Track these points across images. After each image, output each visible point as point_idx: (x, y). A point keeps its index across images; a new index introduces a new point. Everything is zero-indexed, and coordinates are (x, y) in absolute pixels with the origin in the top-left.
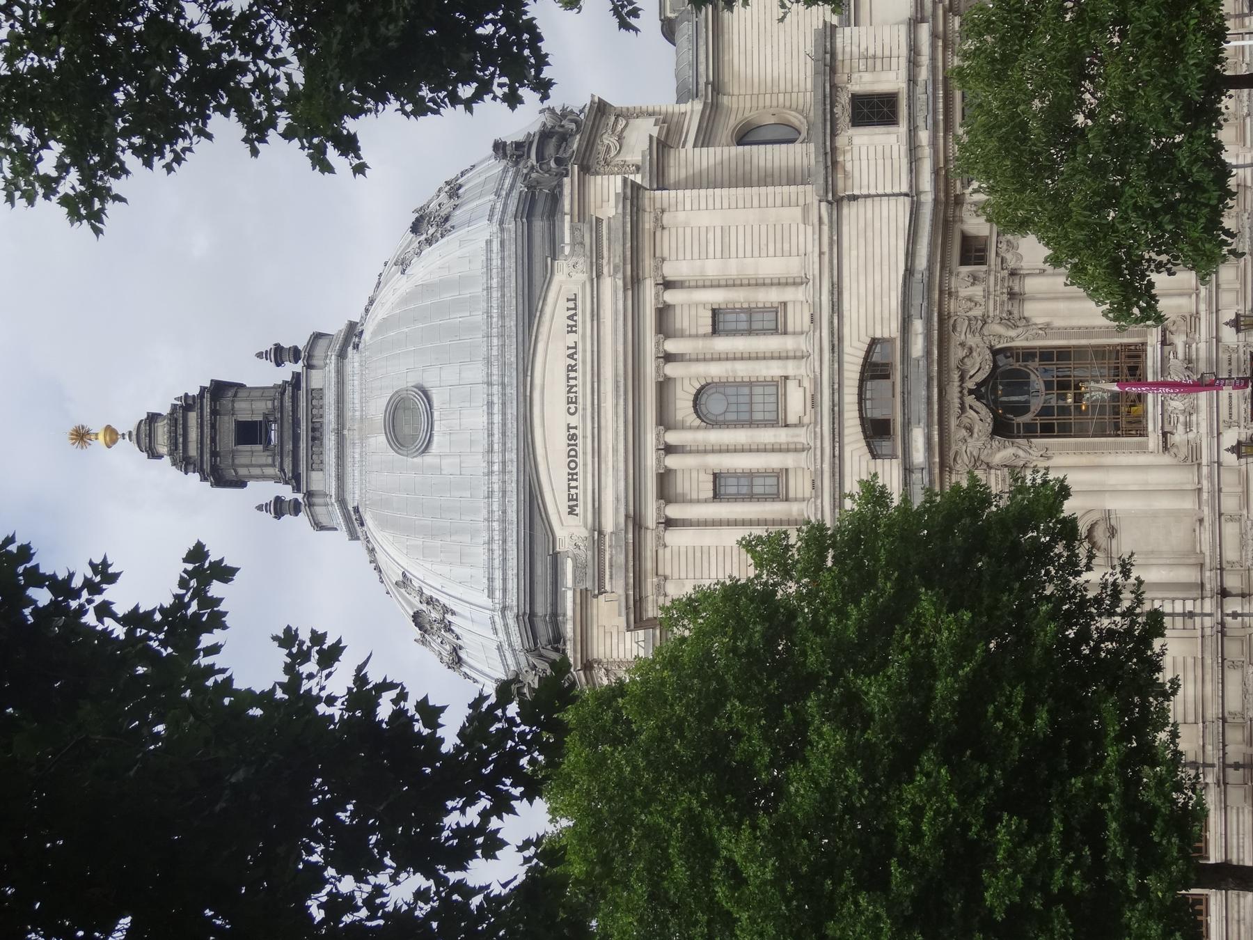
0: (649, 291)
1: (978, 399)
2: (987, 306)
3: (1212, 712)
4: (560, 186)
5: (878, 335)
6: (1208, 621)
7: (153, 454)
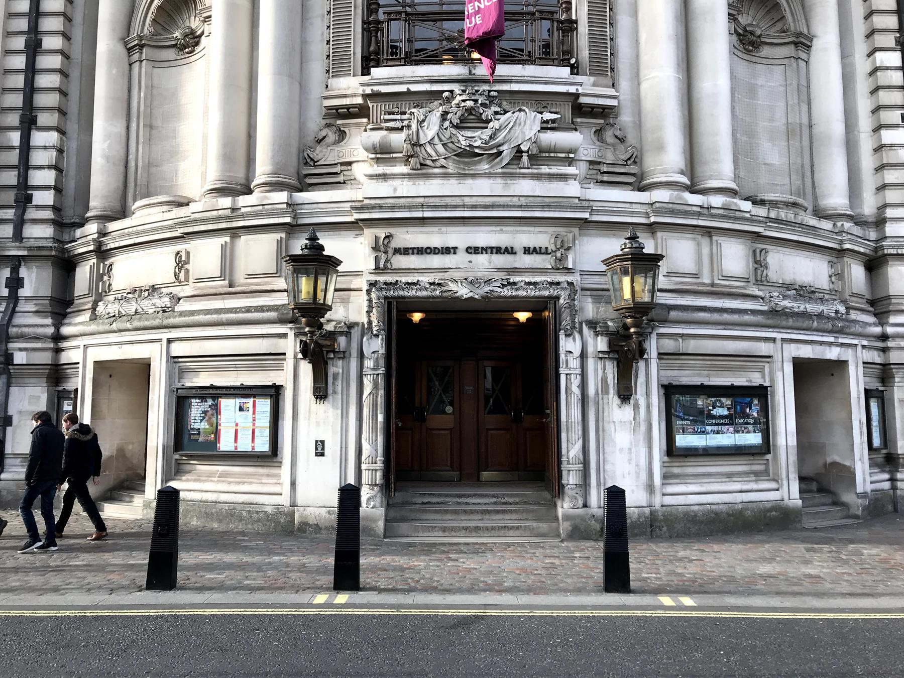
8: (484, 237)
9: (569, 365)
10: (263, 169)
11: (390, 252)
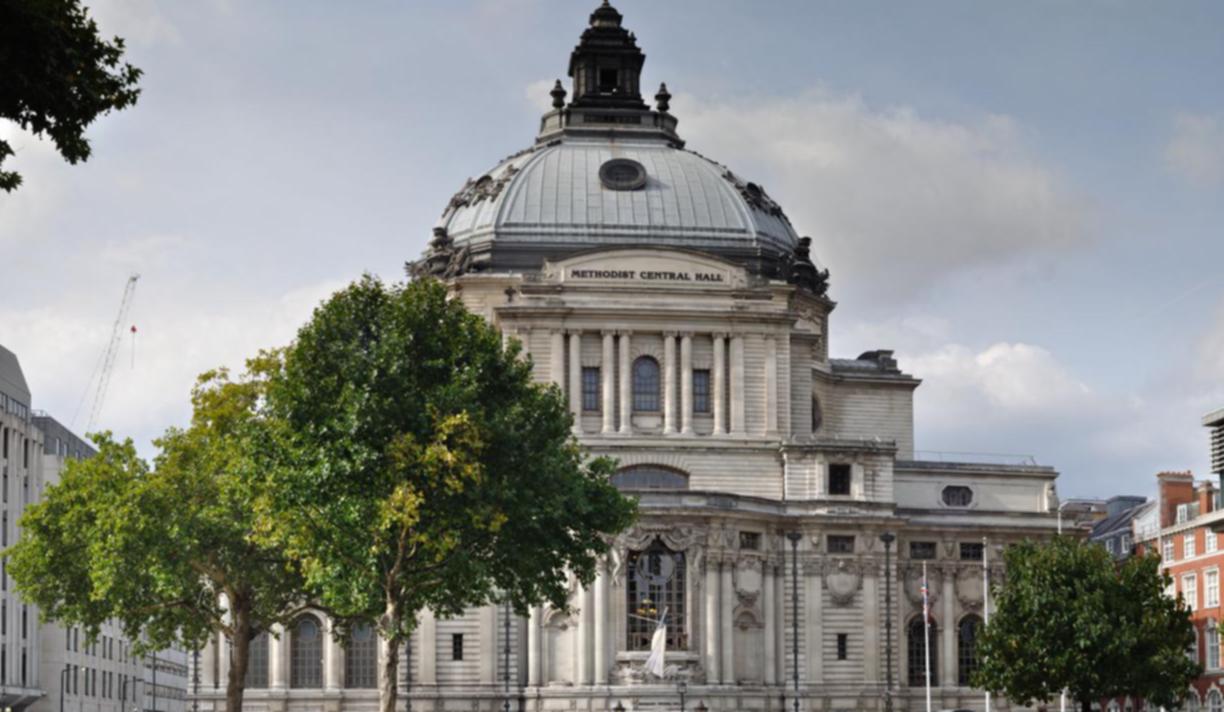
0: (724, 328)
1: (654, 542)
3: (445, 692)
4: (781, 279)
5: (692, 478)
6: (503, 689)
7: (593, 18)
8: (663, 700)
10: (598, 678)
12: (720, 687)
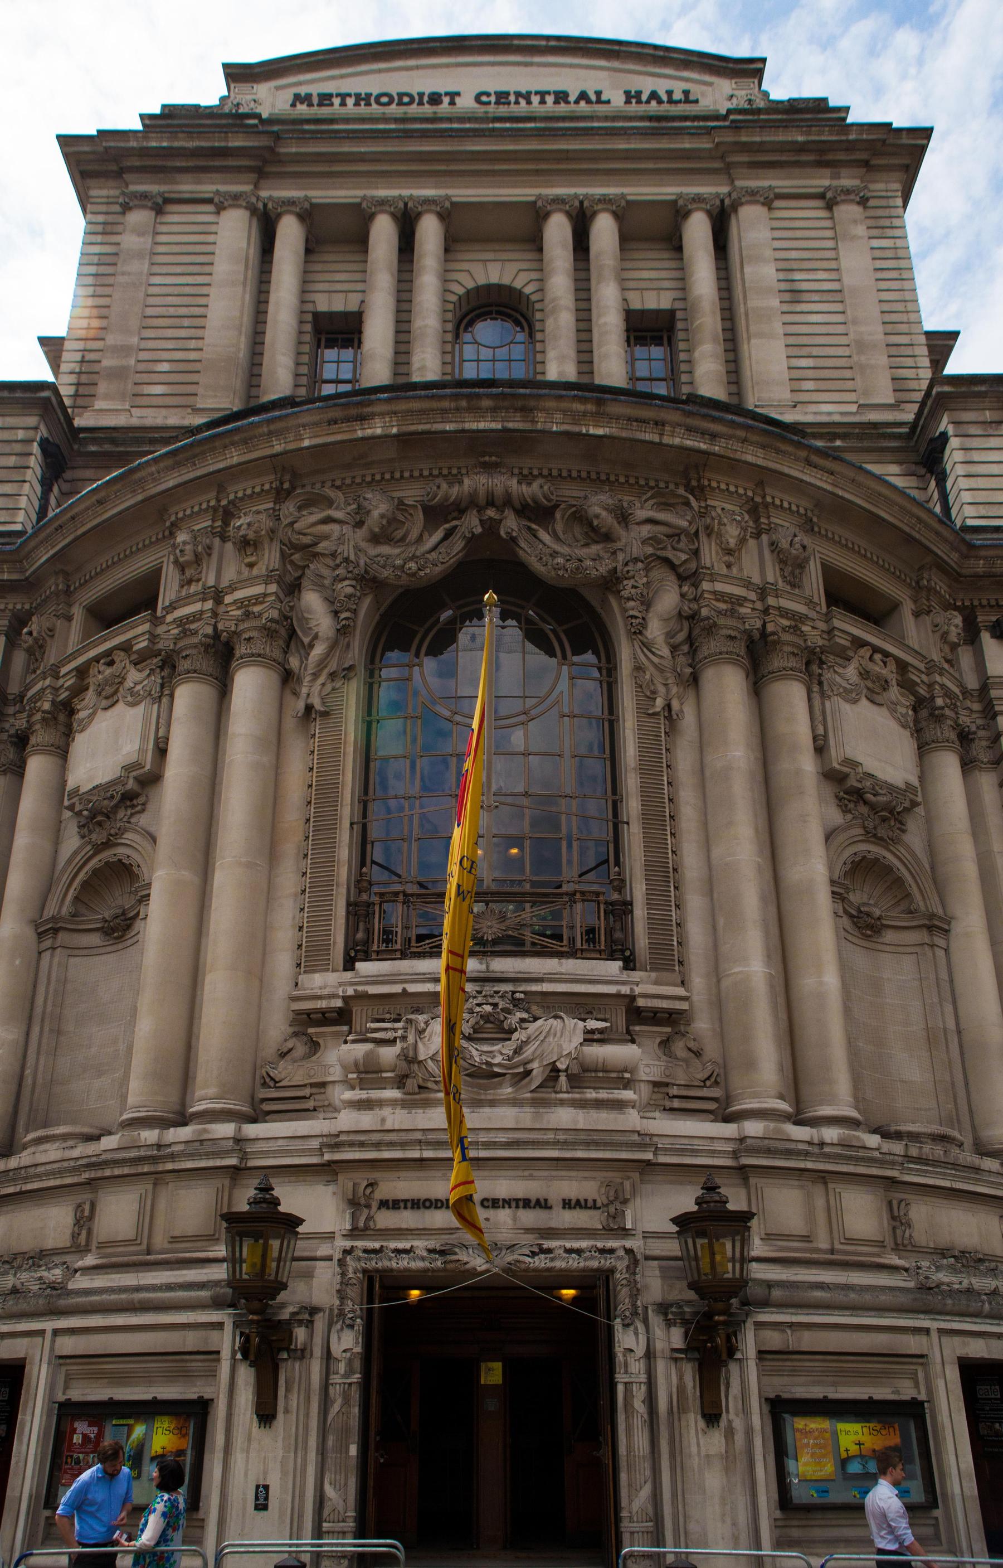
2: (727, 578)
9: (630, 1372)
11: (375, 1205)
12: (800, 1133)
